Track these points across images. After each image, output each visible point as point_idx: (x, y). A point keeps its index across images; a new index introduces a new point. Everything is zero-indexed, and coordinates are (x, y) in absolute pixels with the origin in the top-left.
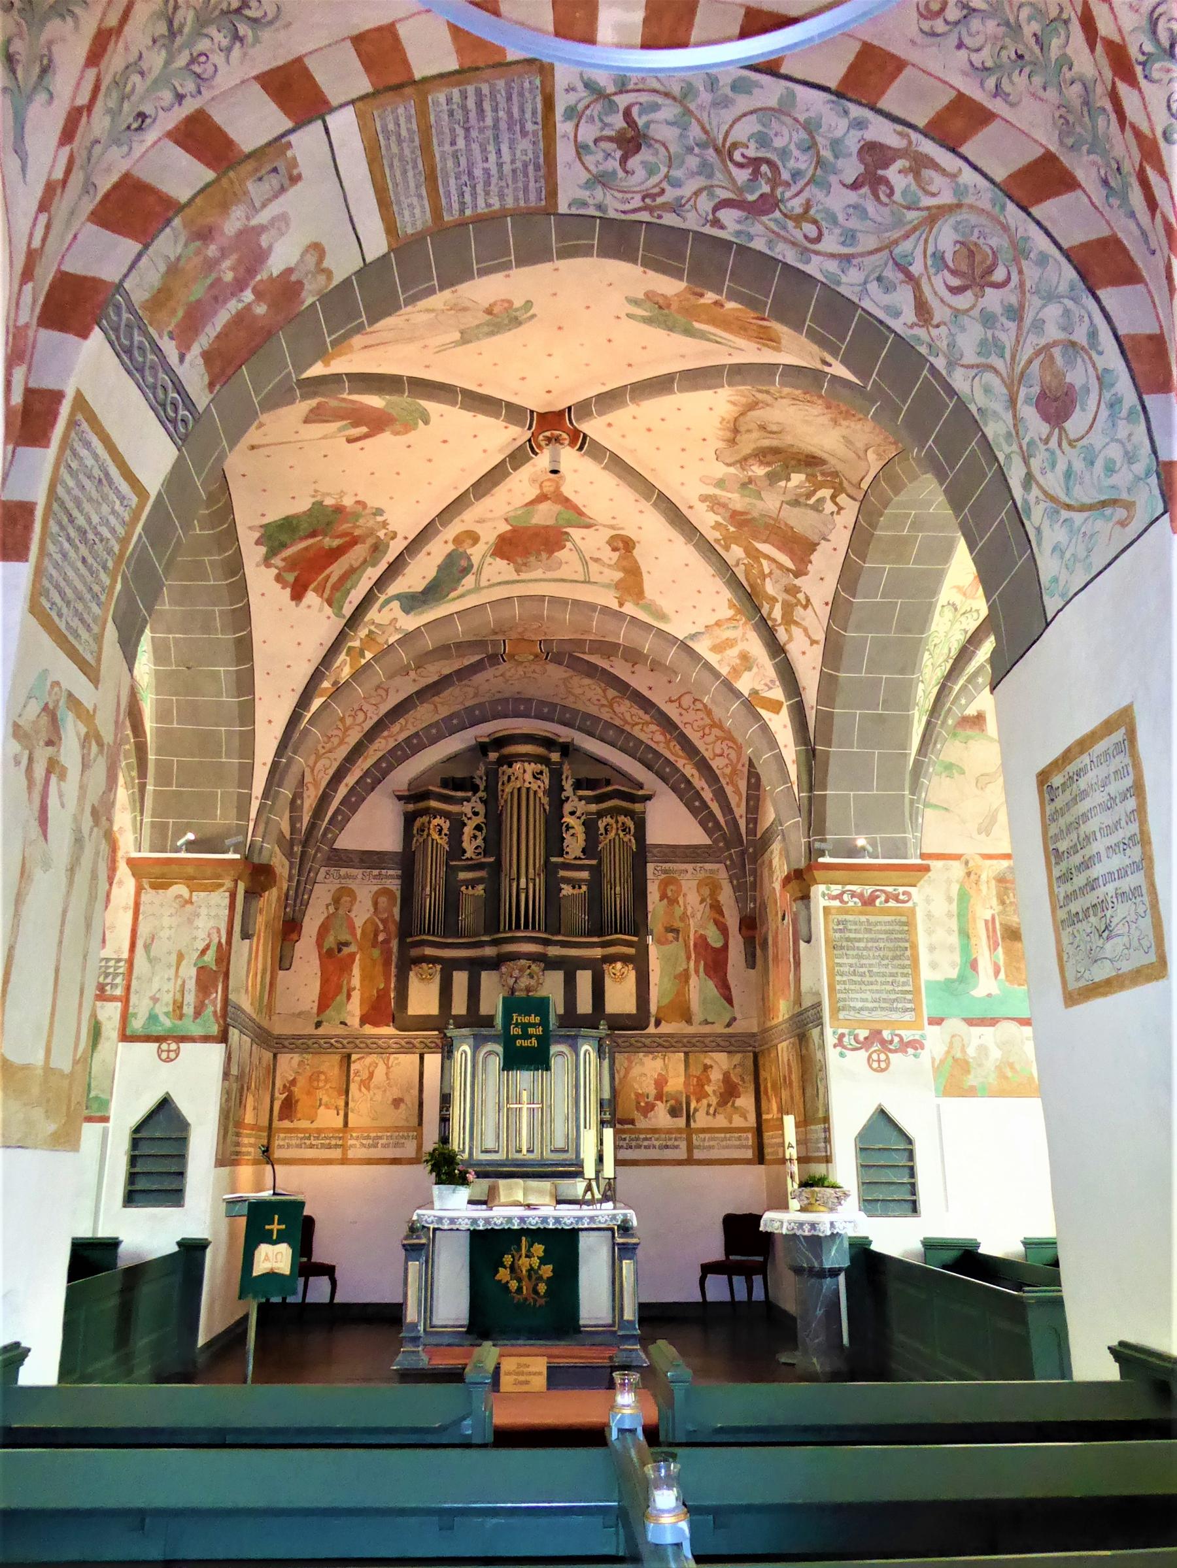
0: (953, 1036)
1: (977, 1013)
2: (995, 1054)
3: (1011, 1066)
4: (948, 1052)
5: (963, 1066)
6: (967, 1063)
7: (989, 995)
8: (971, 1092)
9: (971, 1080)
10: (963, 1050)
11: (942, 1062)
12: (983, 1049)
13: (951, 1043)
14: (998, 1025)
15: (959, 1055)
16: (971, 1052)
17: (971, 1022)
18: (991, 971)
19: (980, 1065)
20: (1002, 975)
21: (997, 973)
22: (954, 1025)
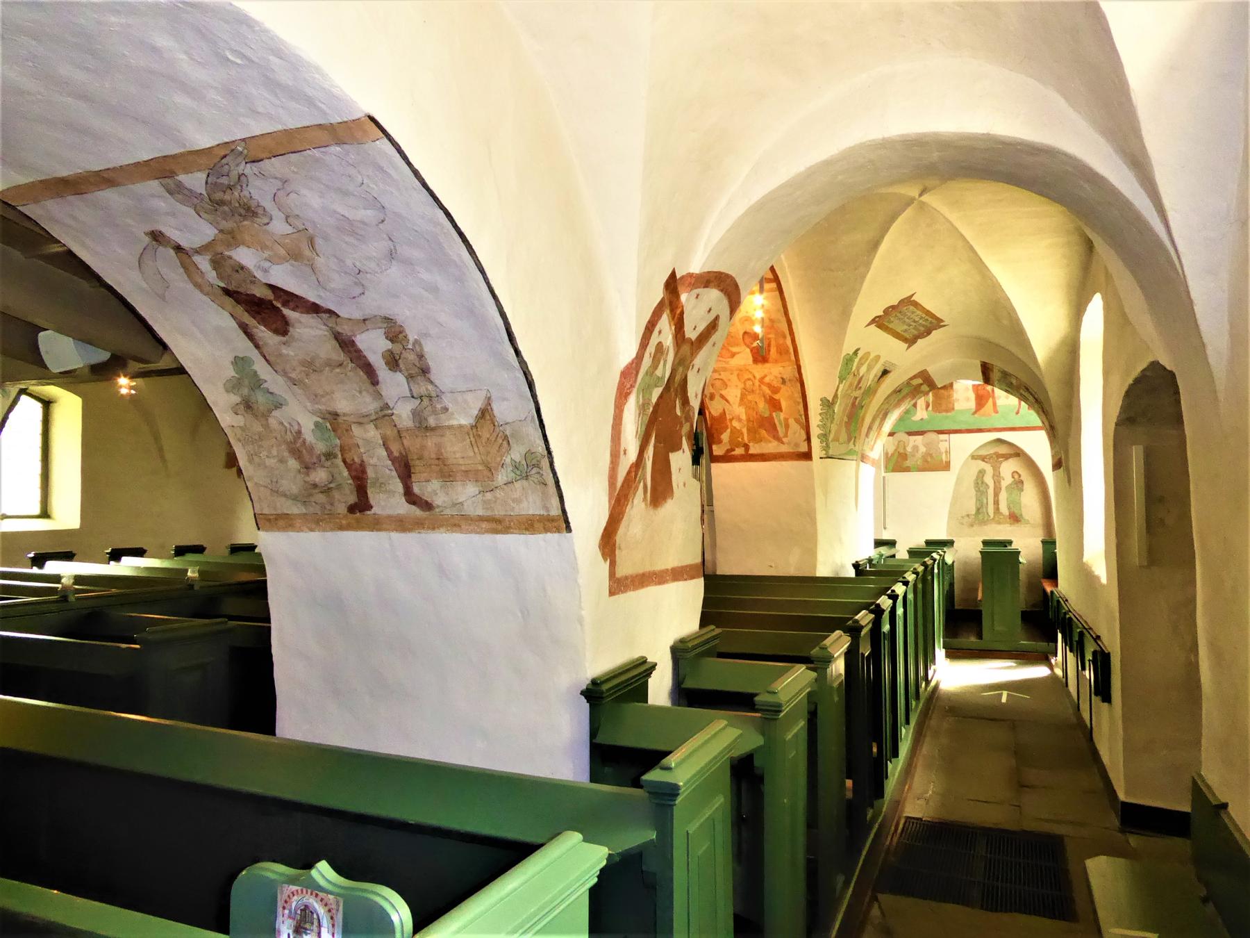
0: (899, 442)
1: (915, 429)
2: (923, 449)
3: (931, 455)
4: (896, 450)
5: (903, 456)
6: (906, 455)
7: (922, 419)
8: (907, 470)
9: (908, 463)
10: (905, 448)
11: (892, 455)
12: (916, 448)
13: (898, 444)
14: (925, 435)
15: (902, 451)
16: (909, 449)
17: (910, 434)
18: (924, 407)
19: (913, 456)
20: (930, 408)
21: (928, 406)
22: (902, 436)
